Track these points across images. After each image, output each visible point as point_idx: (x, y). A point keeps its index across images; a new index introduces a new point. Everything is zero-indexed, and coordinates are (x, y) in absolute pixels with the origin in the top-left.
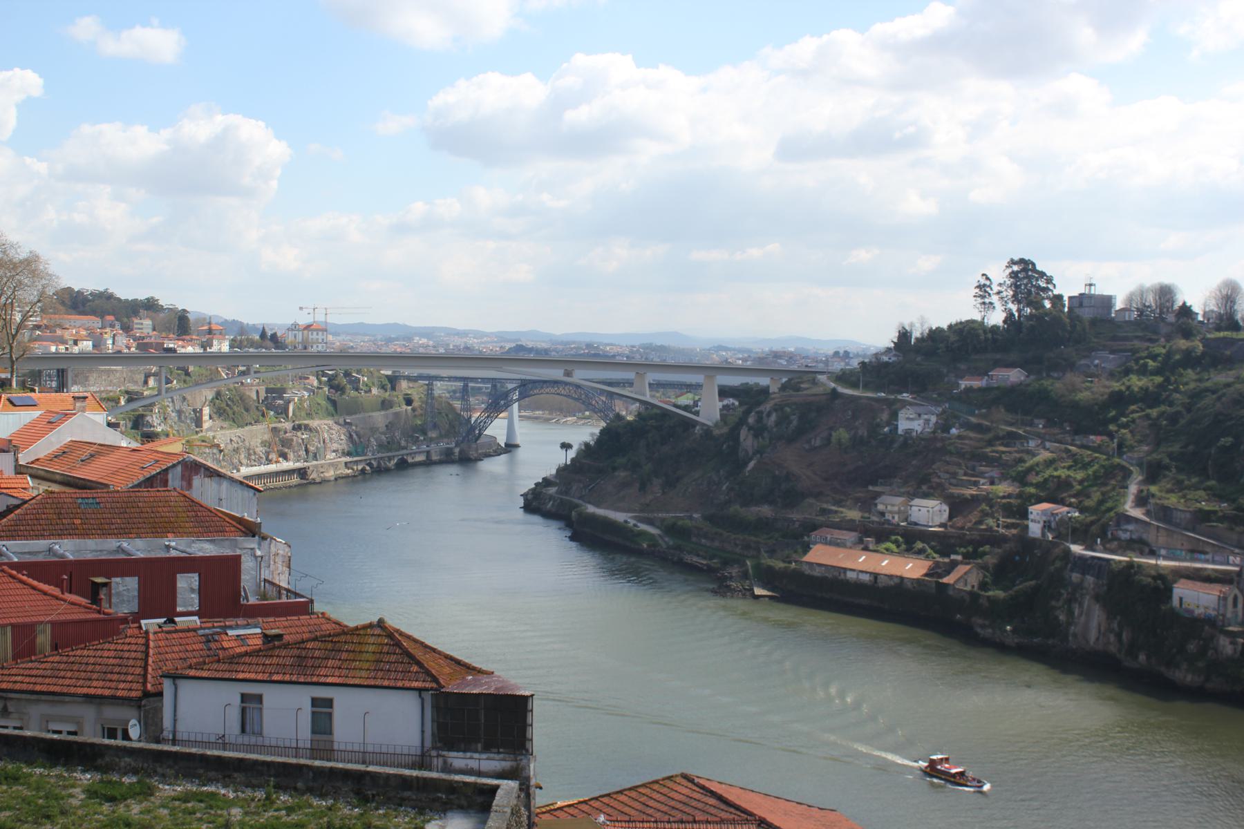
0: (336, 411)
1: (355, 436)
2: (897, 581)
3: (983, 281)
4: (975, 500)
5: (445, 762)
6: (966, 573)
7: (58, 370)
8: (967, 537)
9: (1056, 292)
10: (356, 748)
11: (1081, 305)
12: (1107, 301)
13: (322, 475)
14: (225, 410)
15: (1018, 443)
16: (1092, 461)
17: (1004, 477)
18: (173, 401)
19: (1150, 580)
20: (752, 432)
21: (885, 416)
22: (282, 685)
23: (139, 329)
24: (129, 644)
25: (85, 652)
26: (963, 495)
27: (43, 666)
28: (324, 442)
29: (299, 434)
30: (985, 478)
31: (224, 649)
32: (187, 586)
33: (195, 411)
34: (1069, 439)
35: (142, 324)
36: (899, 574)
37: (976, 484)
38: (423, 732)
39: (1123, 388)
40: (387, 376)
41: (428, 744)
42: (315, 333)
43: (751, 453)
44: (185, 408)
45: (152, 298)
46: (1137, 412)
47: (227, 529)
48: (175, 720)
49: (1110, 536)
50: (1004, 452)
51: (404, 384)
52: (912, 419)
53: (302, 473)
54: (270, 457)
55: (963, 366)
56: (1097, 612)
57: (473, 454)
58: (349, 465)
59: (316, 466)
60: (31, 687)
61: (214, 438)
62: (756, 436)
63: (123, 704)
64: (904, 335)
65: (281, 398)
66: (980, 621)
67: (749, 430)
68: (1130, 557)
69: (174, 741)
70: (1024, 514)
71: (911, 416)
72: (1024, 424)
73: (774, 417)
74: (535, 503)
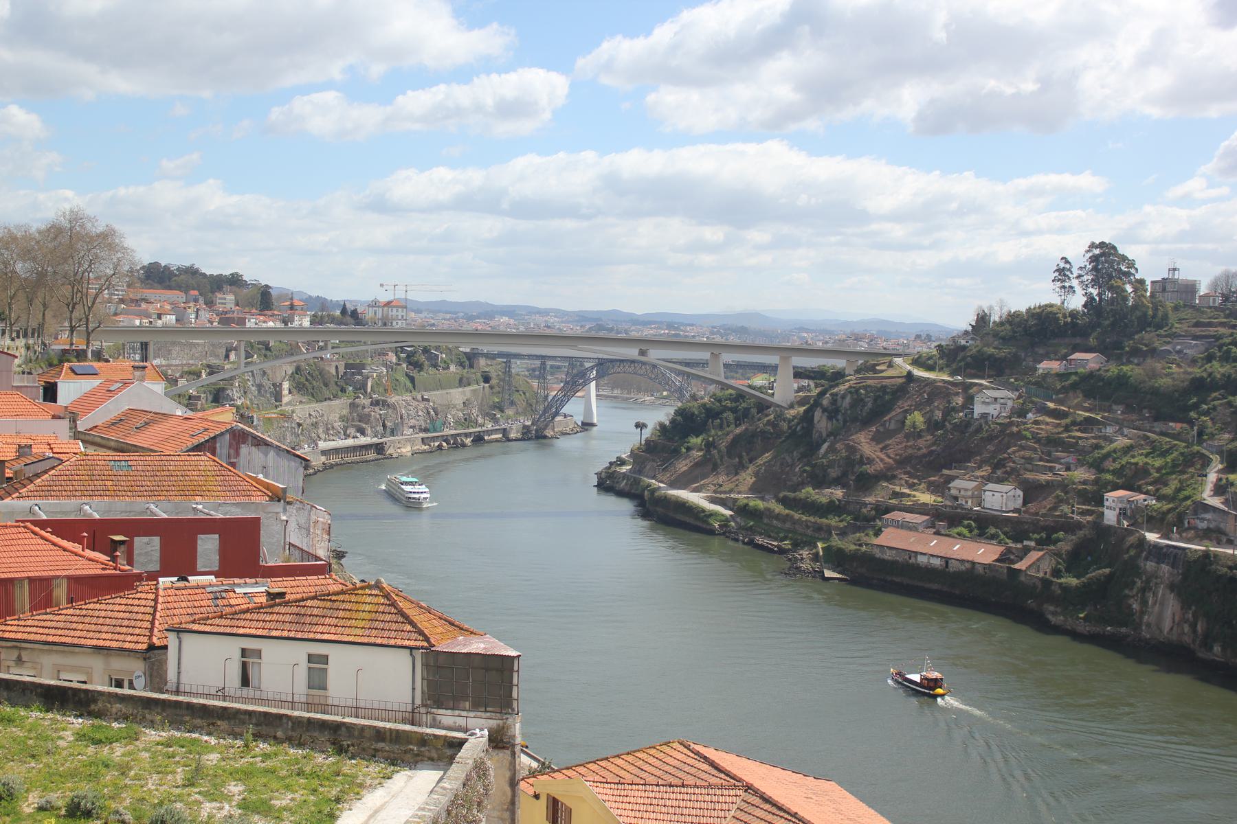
0: (414, 387)
1: (432, 413)
2: (968, 565)
3: (1062, 265)
4: (1049, 486)
5: (434, 719)
6: (1038, 560)
7: (142, 343)
8: (1042, 523)
9: (1138, 277)
10: (349, 704)
11: (1164, 290)
12: (1191, 288)
13: (399, 451)
14: (304, 384)
15: (1095, 428)
16: (1171, 448)
17: (1080, 463)
18: (253, 376)
19: (1225, 570)
20: (826, 414)
21: (959, 400)
22: (280, 641)
23: (222, 304)
24: (139, 599)
25: (98, 606)
26: (1038, 481)
27: (57, 618)
28: (401, 418)
29: (377, 409)
30: (1061, 464)
31: (231, 606)
32: (208, 546)
33: (274, 385)
34: (1148, 426)
35: (225, 299)
36: (970, 559)
37: (1051, 469)
38: (414, 689)
39: (1205, 375)
40: (465, 353)
41: (418, 701)
42: (395, 310)
43: (824, 435)
44: (265, 382)
45: (237, 273)
46: (1219, 399)
47: (254, 493)
48: (179, 673)
49: (1186, 525)
50: (1080, 438)
51: (482, 362)
52: (988, 403)
53: (379, 448)
54: (348, 432)
55: (1041, 351)
56: (1171, 602)
57: (549, 433)
58: (426, 441)
59: (393, 442)
60: (44, 638)
61: (293, 412)
62: (830, 418)
63: (129, 656)
64: (982, 319)
65: (361, 374)
66: (1052, 608)
67: (823, 412)
68: (1206, 546)
69: (177, 692)
70: (1100, 502)
71: (987, 400)
72: (1102, 410)
73: (848, 399)
74: (608, 483)
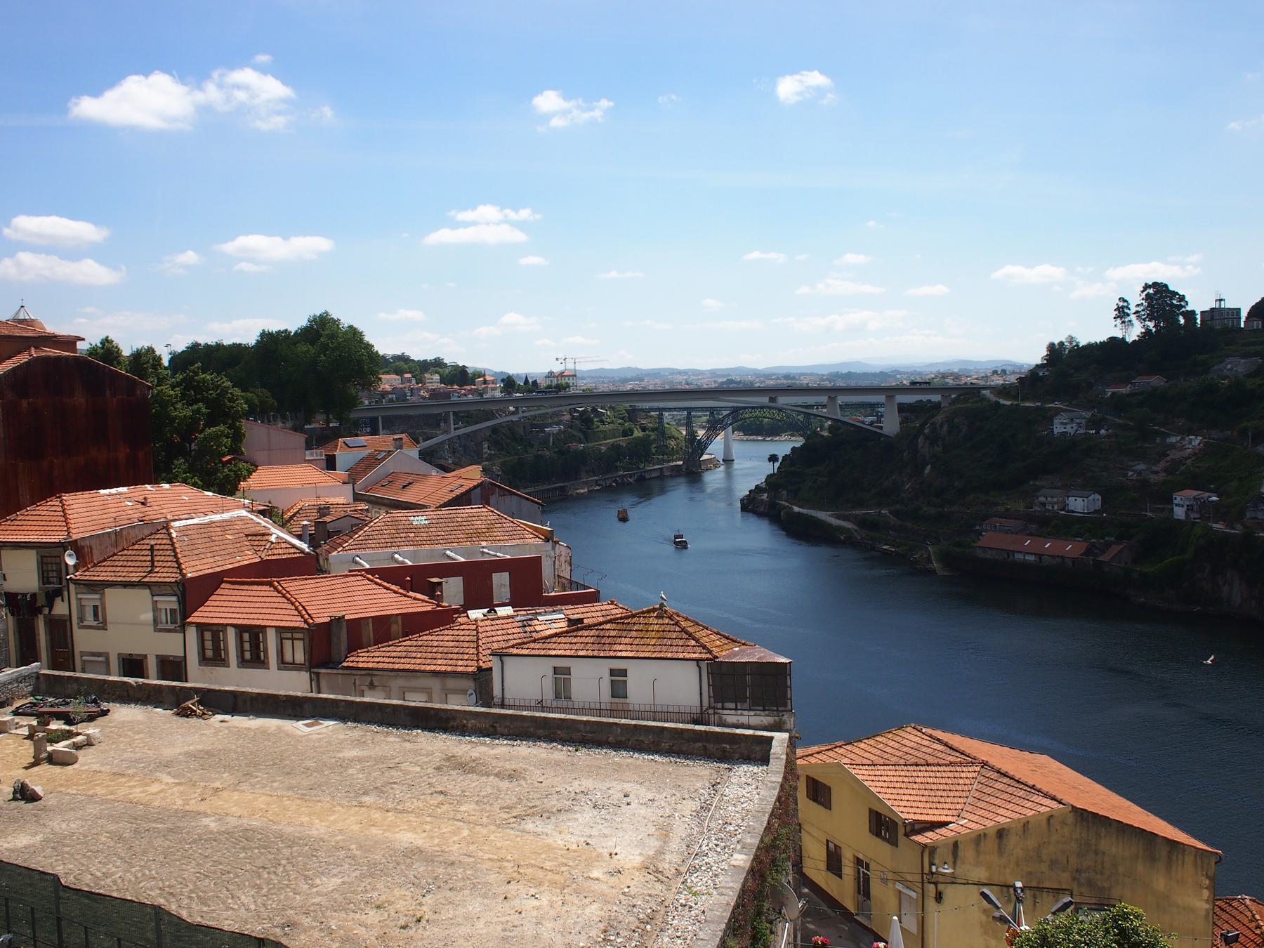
0: (587, 440)
2: (1059, 560)
3: (1121, 304)
5: (720, 718)
6: (1119, 552)
9: (1189, 308)
10: (648, 709)
11: (1212, 318)
23: (431, 383)
24: (463, 630)
25: (430, 638)
27: (399, 649)
31: (536, 631)
32: (501, 580)
35: (432, 379)
38: (701, 694)
41: (706, 703)
42: (567, 378)
45: (439, 358)
47: (527, 536)
48: (503, 690)
53: (562, 489)
60: (391, 666)
63: (462, 677)
69: (503, 706)
70: (1170, 501)
71: (1065, 421)
73: (945, 428)
